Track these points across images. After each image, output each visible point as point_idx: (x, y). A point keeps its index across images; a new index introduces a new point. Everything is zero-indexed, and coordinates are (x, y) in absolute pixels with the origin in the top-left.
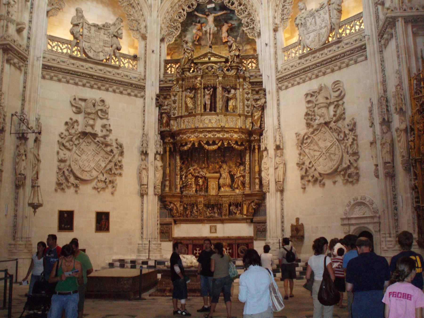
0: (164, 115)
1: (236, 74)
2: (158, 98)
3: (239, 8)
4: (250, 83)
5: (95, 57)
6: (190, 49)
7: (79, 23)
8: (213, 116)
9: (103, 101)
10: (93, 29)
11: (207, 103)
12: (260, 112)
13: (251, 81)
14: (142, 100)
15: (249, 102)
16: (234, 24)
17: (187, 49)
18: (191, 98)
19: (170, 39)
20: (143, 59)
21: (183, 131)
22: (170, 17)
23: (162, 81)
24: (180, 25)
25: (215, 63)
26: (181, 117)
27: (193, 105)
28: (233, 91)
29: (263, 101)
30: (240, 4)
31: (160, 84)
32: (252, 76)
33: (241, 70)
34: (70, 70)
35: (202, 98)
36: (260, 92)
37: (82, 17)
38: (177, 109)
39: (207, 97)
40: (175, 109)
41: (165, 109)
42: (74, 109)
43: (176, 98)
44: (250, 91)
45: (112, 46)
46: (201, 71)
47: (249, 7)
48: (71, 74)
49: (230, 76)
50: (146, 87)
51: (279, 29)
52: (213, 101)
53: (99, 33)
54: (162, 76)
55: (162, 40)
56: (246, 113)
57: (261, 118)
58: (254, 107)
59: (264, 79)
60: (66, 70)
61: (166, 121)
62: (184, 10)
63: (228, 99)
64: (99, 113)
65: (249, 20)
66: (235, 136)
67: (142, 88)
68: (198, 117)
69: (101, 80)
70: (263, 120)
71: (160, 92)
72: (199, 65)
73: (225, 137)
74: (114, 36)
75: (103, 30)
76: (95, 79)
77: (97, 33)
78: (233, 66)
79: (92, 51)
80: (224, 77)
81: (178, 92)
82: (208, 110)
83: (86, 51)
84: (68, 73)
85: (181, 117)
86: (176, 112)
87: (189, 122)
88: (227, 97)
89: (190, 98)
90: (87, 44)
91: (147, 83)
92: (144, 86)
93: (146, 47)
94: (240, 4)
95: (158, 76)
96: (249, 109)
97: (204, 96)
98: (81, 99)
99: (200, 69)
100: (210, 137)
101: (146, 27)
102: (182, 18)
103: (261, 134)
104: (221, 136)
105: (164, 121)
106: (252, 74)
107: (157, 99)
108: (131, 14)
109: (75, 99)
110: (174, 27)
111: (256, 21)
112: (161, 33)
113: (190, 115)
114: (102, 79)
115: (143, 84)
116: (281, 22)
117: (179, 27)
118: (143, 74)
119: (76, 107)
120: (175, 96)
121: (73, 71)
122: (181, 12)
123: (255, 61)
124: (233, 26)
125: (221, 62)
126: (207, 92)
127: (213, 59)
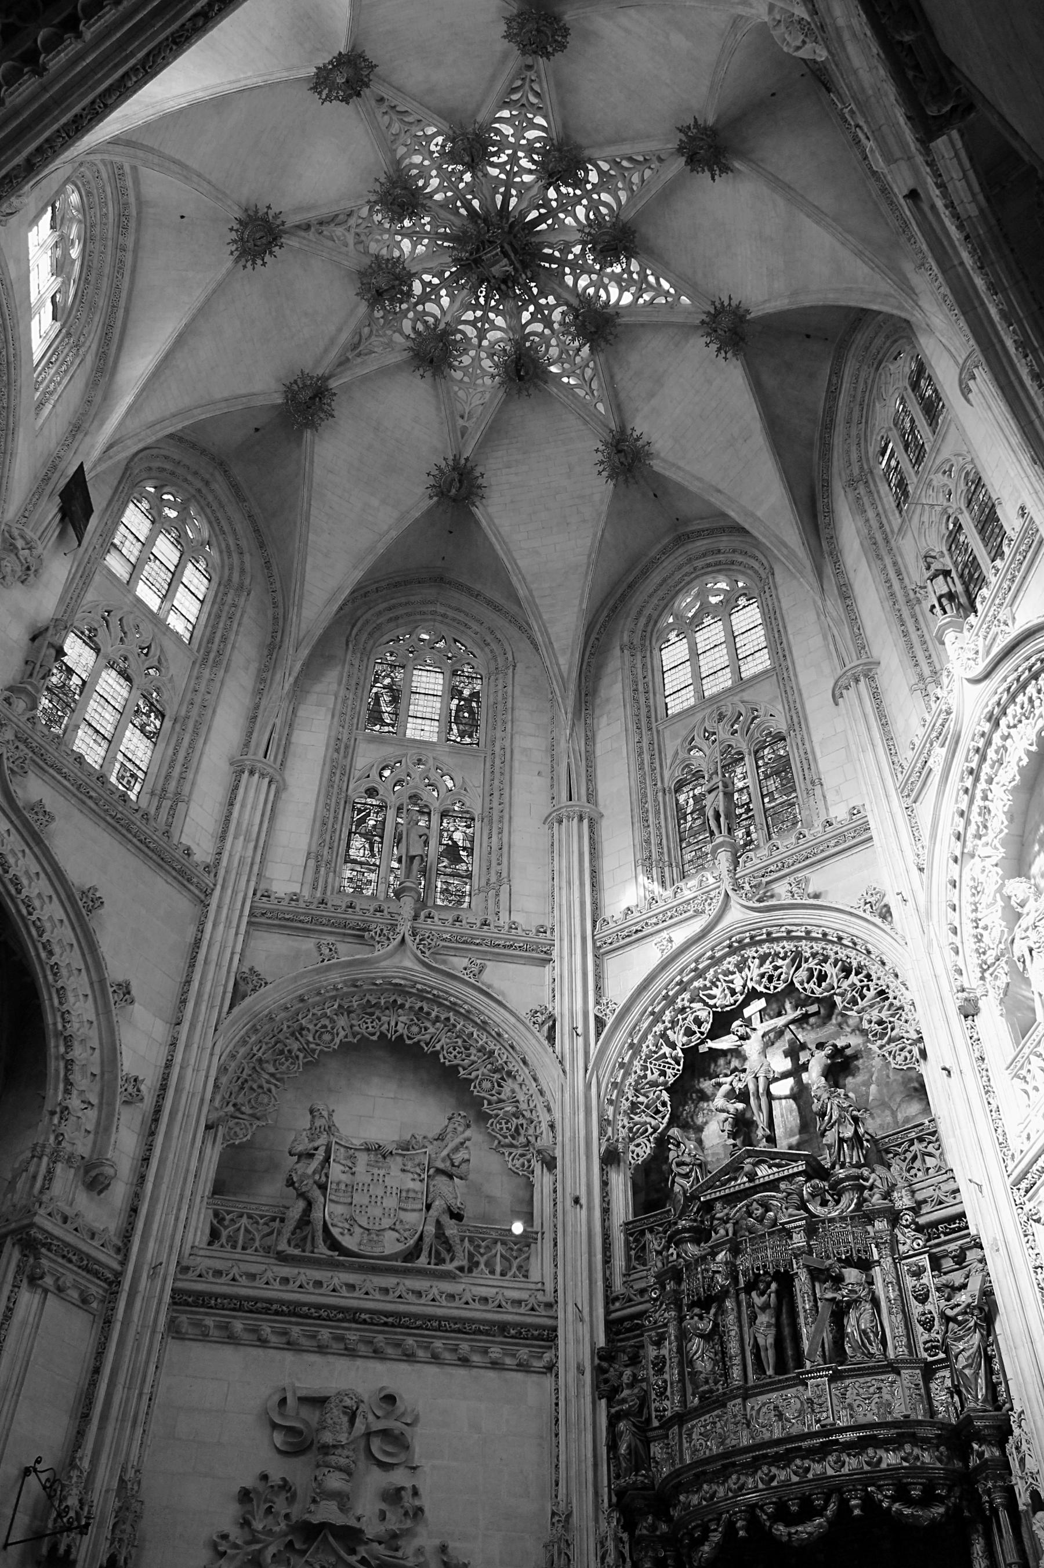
0: (622, 1426)
1: (859, 1205)
2: (605, 1365)
3: (845, 984)
4: (919, 1229)
5: (367, 1250)
6: (688, 1160)
7: (316, 1149)
8: (790, 1392)
9: (390, 1399)
10: (362, 1158)
11: (761, 1341)
12: (977, 1335)
13: (921, 1221)
14: (548, 1381)
15: (929, 1307)
16: (848, 1046)
17: (680, 1164)
18: (706, 1337)
19: (638, 1150)
20: (549, 1236)
21: (684, 1478)
22: (632, 1079)
23: (617, 1299)
24: (665, 1096)
25: (772, 1185)
26: (680, 1419)
27: (716, 1363)
28: (852, 1275)
29: (975, 1285)
30: (847, 971)
31: (607, 1313)
32: (920, 1204)
33: (871, 1188)
34: (270, 1301)
35: (746, 1329)
36: (971, 1255)
37: (330, 1129)
38: (668, 1393)
39: (763, 1319)
40: (662, 1394)
41: (624, 1401)
42: (278, 1438)
43: (664, 1352)
44: (925, 1261)
45: (428, 1207)
46: (730, 1226)
47: (874, 970)
48: (277, 1313)
49: (832, 1220)
50: (560, 1332)
51: (981, 1004)
52: (786, 1331)
53: (382, 1172)
54: (618, 1282)
55: (611, 1158)
56: (925, 1355)
57: (989, 1359)
58: (948, 1319)
59: (970, 1203)
60: (256, 1300)
61: (629, 1447)
62: (673, 1046)
63: (839, 1312)
64: (376, 1445)
65: (884, 1015)
66: (890, 1459)
67: (548, 1336)
68: (734, 1406)
69: (385, 1324)
70: (997, 1367)
71: (608, 1340)
72: (718, 1205)
73: (845, 1470)
74: (439, 1171)
75: (399, 1159)
76: (365, 1322)
77: (376, 1171)
78: (843, 1180)
79: (357, 1230)
80: (811, 1231)
81: (665, 1325)
82: (770, 1372)
83: (335, 1231)
84: (266, 1311)
85: (680, 1419)
86: (667, 1403)
87: (705, 1435)
88: (833, 1299)
89: (701, 1336)
90: (339, 1209)
91: (561, 1315)
92: (555, 1329)
93: (555, 1191)
94: (847, 971)
95: (600, 1284)
96: (934, 1335)
97: (753, 1318)
98: (303, 1400)
99: (725, 1221)
100: (786, 1484)
101: (552, 1126)
102: (669, 1071)
103: (1002, 1432)
104: (830, 1472)
105: (623, 1449)
106: (920, 1196)
107: (599, 1371)
108: (502, 1096)
109: (283, 1401)
110: (647, 1107)
111: (907, 1008)
112: (602, 1132)
113: (712, 1402)
114: (390, 1320)
115: (549, 1322)
116: (983, 978)
117: (664, 1104)
118: (549, 1287)
119: (290, 1430)
120: (658, 1344)
121: (282, 1302)
122: (664, 1056)
123: (931, 1149)
124: (848, 1052)
125: (790, 1178)
126: (758, 1300)
127: (763, 1172)
